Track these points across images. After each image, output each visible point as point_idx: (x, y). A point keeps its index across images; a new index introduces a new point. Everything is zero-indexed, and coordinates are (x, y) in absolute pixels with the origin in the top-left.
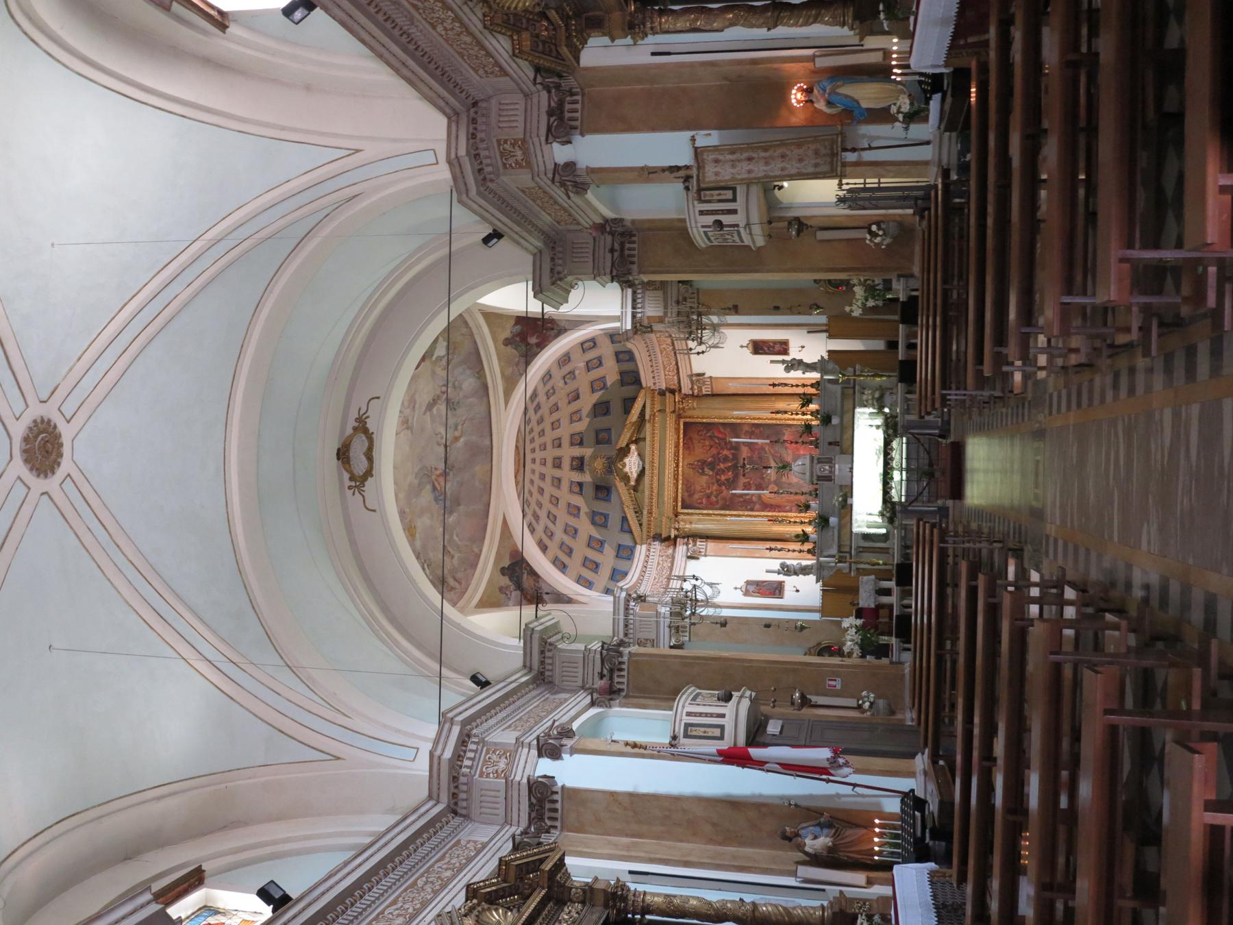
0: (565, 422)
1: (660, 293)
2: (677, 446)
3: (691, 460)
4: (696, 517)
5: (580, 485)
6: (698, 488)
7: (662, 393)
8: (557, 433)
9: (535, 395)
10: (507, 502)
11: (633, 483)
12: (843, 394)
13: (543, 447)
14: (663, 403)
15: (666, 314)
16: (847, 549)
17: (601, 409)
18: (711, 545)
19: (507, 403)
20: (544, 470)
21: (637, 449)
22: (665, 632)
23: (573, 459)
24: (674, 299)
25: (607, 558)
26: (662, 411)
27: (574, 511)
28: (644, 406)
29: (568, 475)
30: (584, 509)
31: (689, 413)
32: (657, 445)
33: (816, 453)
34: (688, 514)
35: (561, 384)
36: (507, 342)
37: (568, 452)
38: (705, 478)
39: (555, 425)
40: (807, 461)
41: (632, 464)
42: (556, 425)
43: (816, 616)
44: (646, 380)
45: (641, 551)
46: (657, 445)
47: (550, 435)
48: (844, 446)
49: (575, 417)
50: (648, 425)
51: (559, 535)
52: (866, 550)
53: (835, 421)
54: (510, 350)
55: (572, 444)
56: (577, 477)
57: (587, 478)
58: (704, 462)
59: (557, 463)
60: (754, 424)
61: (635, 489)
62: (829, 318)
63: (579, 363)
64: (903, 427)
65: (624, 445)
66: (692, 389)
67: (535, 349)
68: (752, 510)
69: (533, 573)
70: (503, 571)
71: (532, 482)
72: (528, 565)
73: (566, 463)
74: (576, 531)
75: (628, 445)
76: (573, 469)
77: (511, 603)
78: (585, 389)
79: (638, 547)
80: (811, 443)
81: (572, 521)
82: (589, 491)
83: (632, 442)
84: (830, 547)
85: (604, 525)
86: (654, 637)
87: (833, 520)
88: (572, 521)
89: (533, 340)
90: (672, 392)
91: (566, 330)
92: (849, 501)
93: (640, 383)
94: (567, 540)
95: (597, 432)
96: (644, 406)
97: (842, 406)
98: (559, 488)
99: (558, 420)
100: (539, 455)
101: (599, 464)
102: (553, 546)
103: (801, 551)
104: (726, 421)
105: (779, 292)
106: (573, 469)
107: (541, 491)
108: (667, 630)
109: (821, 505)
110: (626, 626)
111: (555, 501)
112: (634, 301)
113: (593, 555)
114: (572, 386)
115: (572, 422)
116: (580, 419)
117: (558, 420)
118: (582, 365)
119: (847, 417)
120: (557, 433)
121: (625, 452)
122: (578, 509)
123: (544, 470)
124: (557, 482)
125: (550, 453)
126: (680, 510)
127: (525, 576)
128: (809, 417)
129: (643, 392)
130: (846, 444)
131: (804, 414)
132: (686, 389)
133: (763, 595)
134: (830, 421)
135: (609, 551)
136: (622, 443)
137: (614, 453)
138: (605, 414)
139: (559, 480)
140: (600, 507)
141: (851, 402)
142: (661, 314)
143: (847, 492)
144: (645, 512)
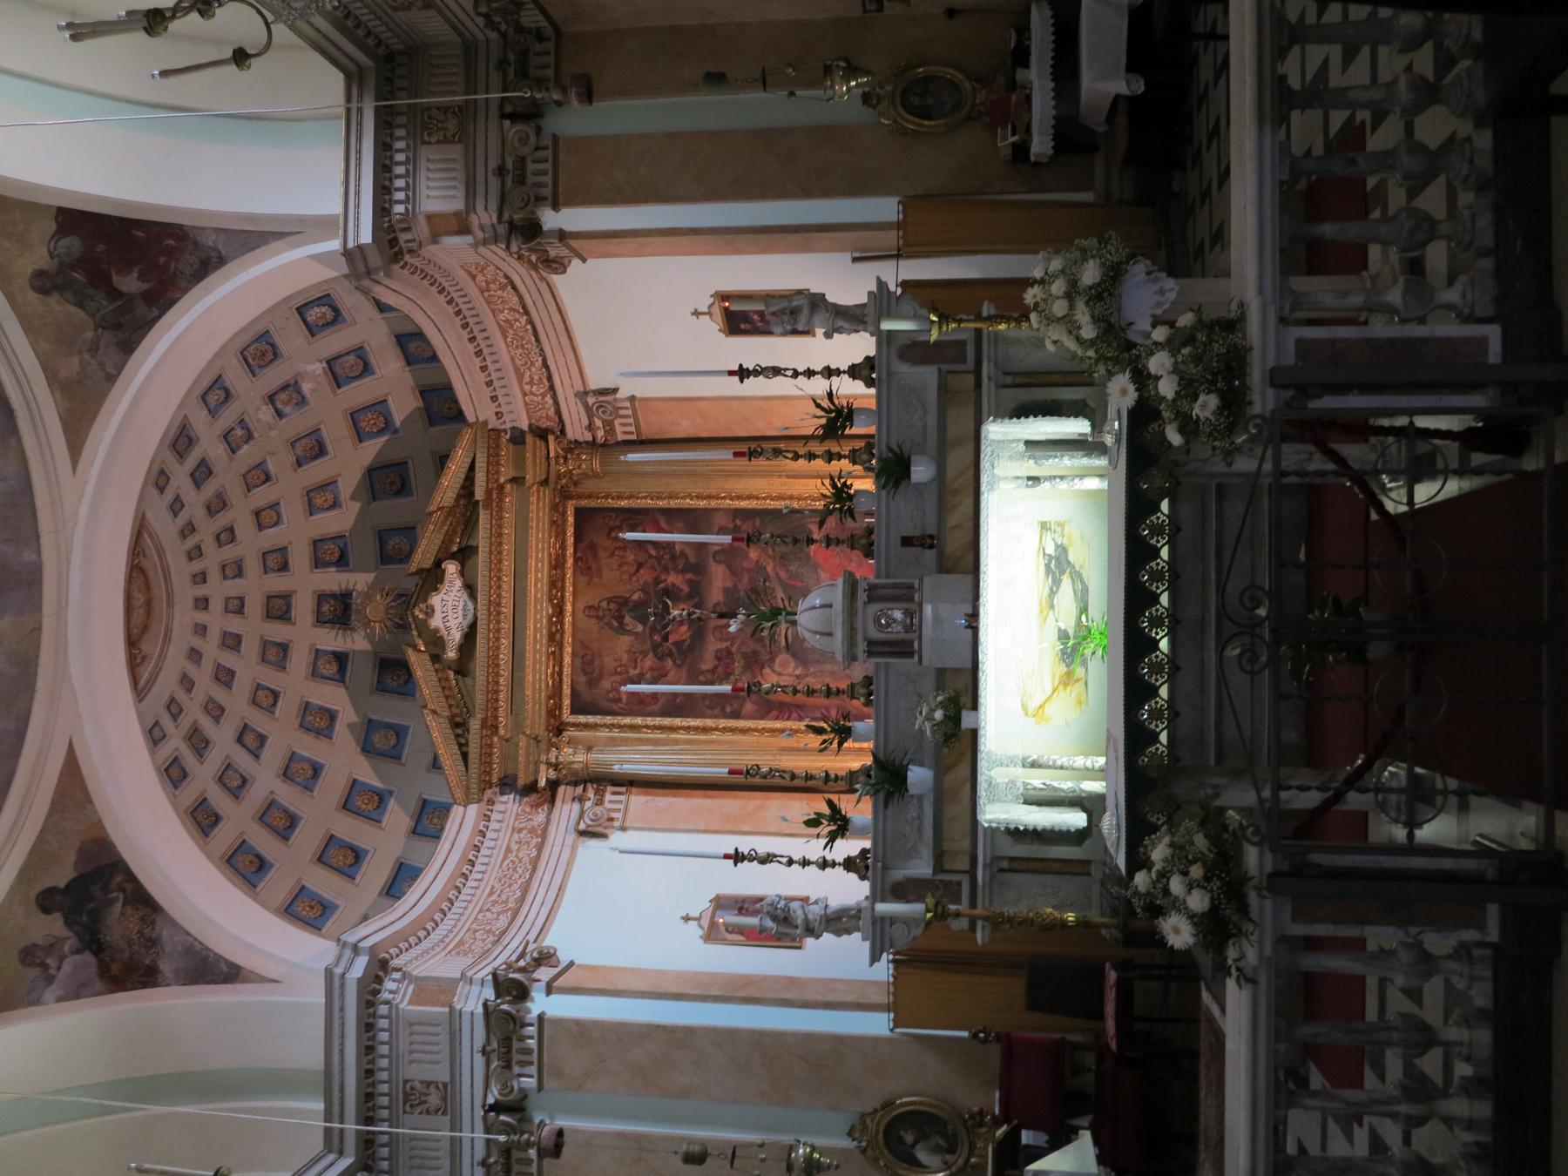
0: (293, 510)
1: (456, 151)
2: (557, 564)
3: (592, 597)
4: (604, 734)
5: (341, 659)
6: (609, 663)
7: (518, 438)
8: (272, 537)
9: (181, 440)
10: (93, 709)
11: (451, 654)
12: (943, 388)
13: (236, 570)
14: (520, 462)
15: (470, 206)
16: (964, 864)
17: (389, 479)
18: (638, 801)
19: (75, 450)
20: (234, 624)
21: (462, 573)
22: (473, 1067)
23: (321, 598)
24: (493, 163)
25: (387, 839)
26: (517, 481)
27: (319, 722)
28: (472, 468)
29: (307, 635)
30: (347, 714)
31: (589, 486)
32: (508, 564)
33: (866, 570)
34: (586, 726)
35: (266, 413)
36: (44, 283)
37: (307, 583)
38: (626, 640)
39: (265, 517)
40: (837, 595)
41: (448, 609)
42: (267, 516)
43: (877, 1024)
44: (474, 402)
45: (463, 820)
46: (508, 564)
47: (250, 543)
48: (948, 550)
49: (319, 497)
50: (483, 516)
51: (266, 780)
52: (1019, 865)
53: (921, 471)
54: (59, 307)
55: (318, 563)
56: (331, 640)
57: (357, 642)
58: (622, 602)
59: (279, 608)
60: (738, 513)
61: (462, 667)
62: (906, 205)
63: (305, 359)
64: (1276, 378)
65: (428, 564)
66: (590, 427)
67: (141, 309)
68: (736, 715)
69: (143, 901)
70: (47, 901)
71: (195, 655)
72: (131, 877)
73: (303, 607)
74: (317, 770)
75: (438, 564)
76: (320, 620)
77: (51, 993)
78: (336, 432)
79: (457, 811)
80: (852, 542)
81: (309, 748)
82: (363, 673)
83: (453, 556)
84: (912, 853)
85: (394, 755)
86: (447, 1078)
87: (919, 776)
88: (309, 748)
89: (130, 283)
90: (542, 434)
91: (222, 261)
92: (967, 722)
93: (459, 416)
94: (287, 795)
95: (382, 536)
96: (472, 468)
97: (942, 427)
98: (281, 666)
99: (274, 506)
100: (218, 589)
101: (376, 609)
102: (238, 821)
103: (824, 864)
104: (673, 504)
105: (765, 138)
106: (320, 620)
107: (225, 677)
108: (479, 1060)
109: (882, 733)
110: (368, 1049)
111: (265, 699)
112: (383, 169)
113: (351, 829)
114: (298, 422)
115: (312, 509)
116: (335, 505)
117: (274, 506)
118: (318, 368)
119: (956, 461)
120: (272, 537)
121: (432, 578)
122: (332, 716)
123: (234, 624)
124: (276, 655)
125: (256, 586)
126: (567, 716)
127: (117, 908)
128: (845, 464)
129: (467, 435)
130: (955, 543)
131: (830, 457)
132: (576, 429)
133: (756, 937)
134: (906, 473)
135: (397, 817)
136: (423, 556)
137: (410, 584)
138: (398, 493)
139: (284, 648)
140: (390, 710)
141: (969, 413)
142: (458, 205)
143: (961, 687)
144: (475, 725)
